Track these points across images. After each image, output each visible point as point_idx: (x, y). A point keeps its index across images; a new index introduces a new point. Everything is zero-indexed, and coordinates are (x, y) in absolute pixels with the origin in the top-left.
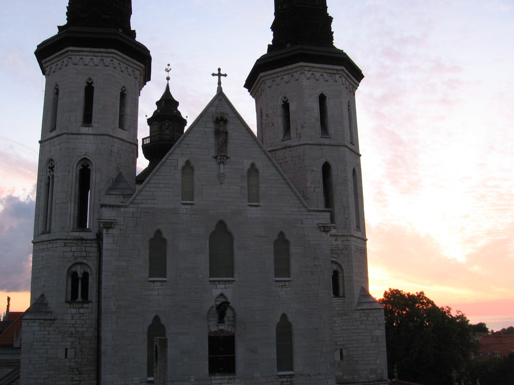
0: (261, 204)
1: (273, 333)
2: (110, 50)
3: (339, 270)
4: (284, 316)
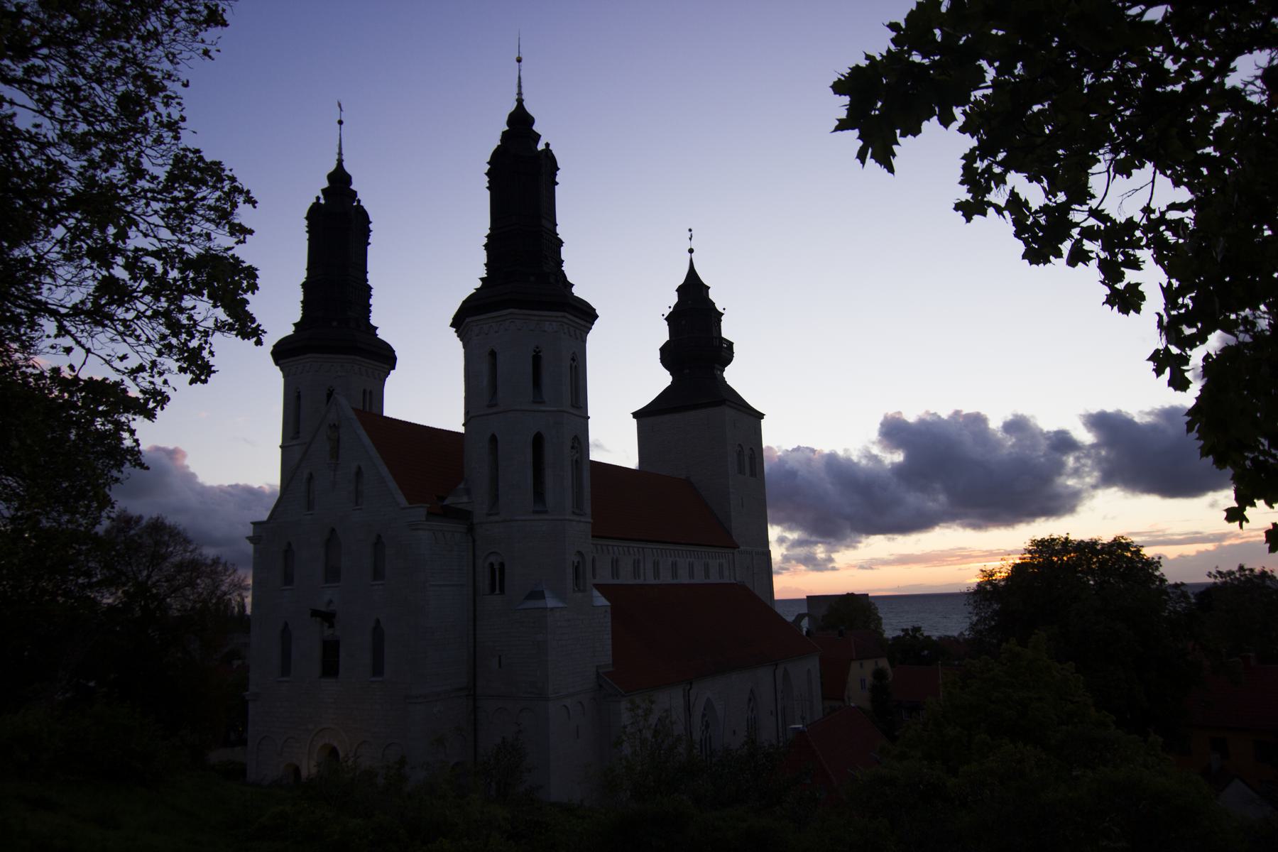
4: (378, 621)
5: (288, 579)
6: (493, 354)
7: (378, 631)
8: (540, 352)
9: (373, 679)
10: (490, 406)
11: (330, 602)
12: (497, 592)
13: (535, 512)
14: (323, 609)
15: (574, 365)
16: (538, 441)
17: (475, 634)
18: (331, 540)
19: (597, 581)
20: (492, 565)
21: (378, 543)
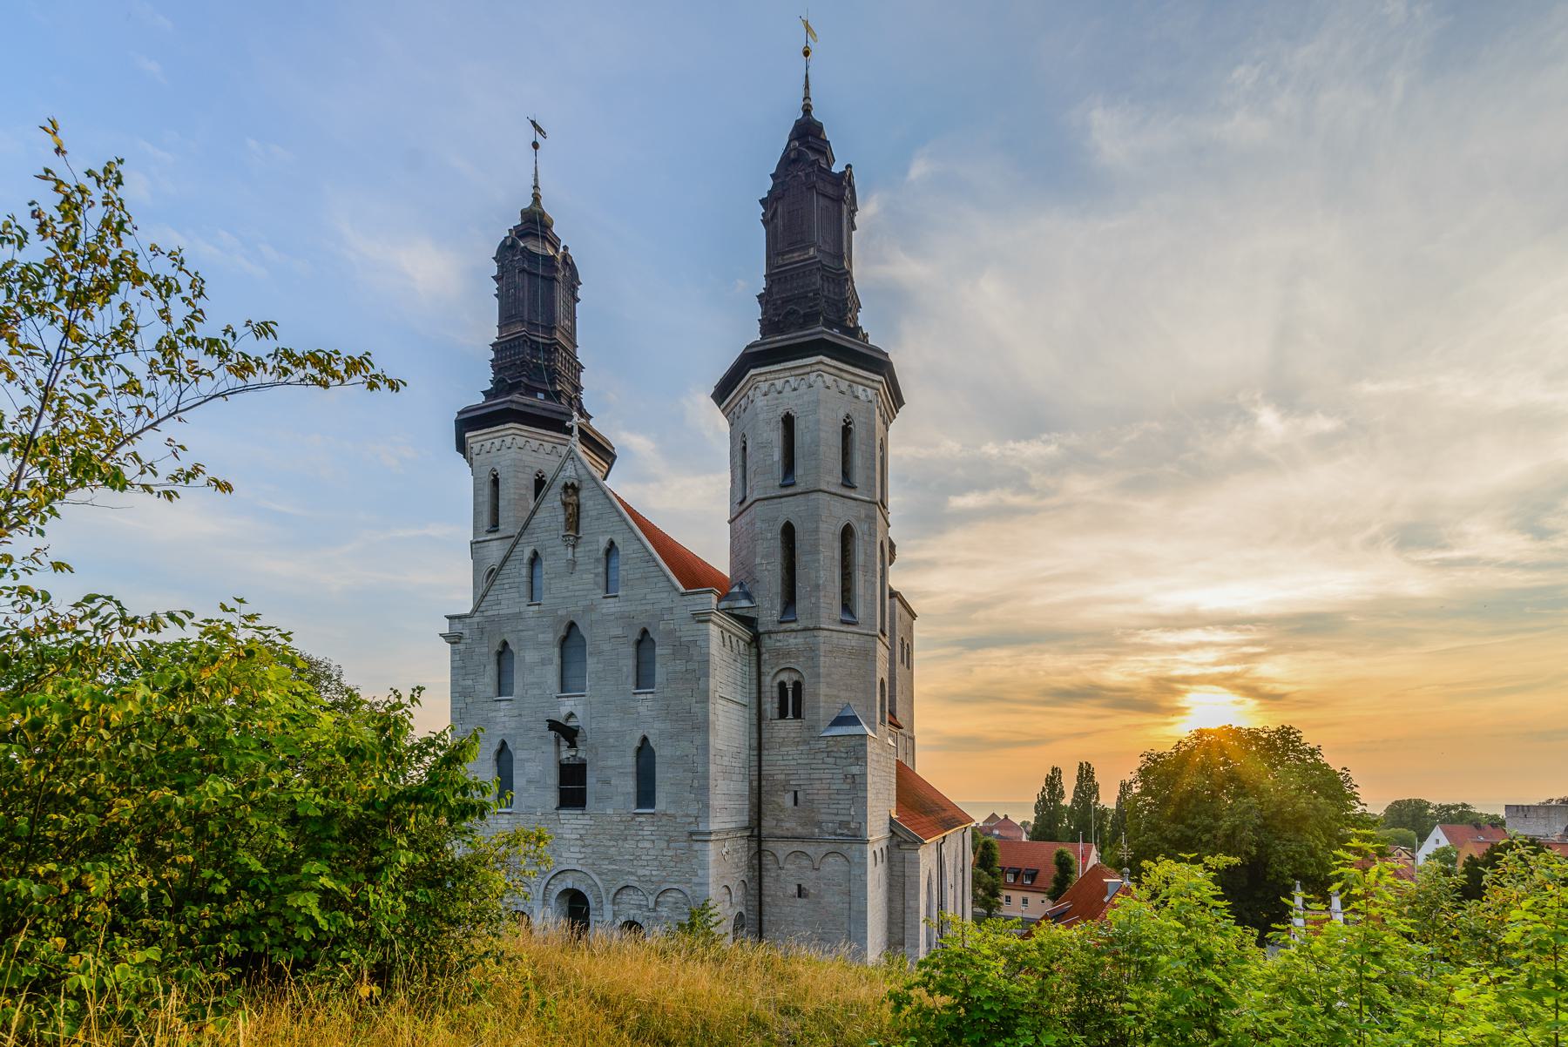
0: (620, 593)
1: (630, 759)
2: (507, 426)
3: (801, 680)
4: (645, 739)
5: (503, 686)
6: (788, 422)
7: (645, 753)
9: (637, 811)
10: (782, 486)
11: (571, 715)
12: (790, 715)
13: (843, 622)
16: (847, 534)
17: (760, 766)
18: (570, 639)
20: (782, 685)
21: (644, 641)
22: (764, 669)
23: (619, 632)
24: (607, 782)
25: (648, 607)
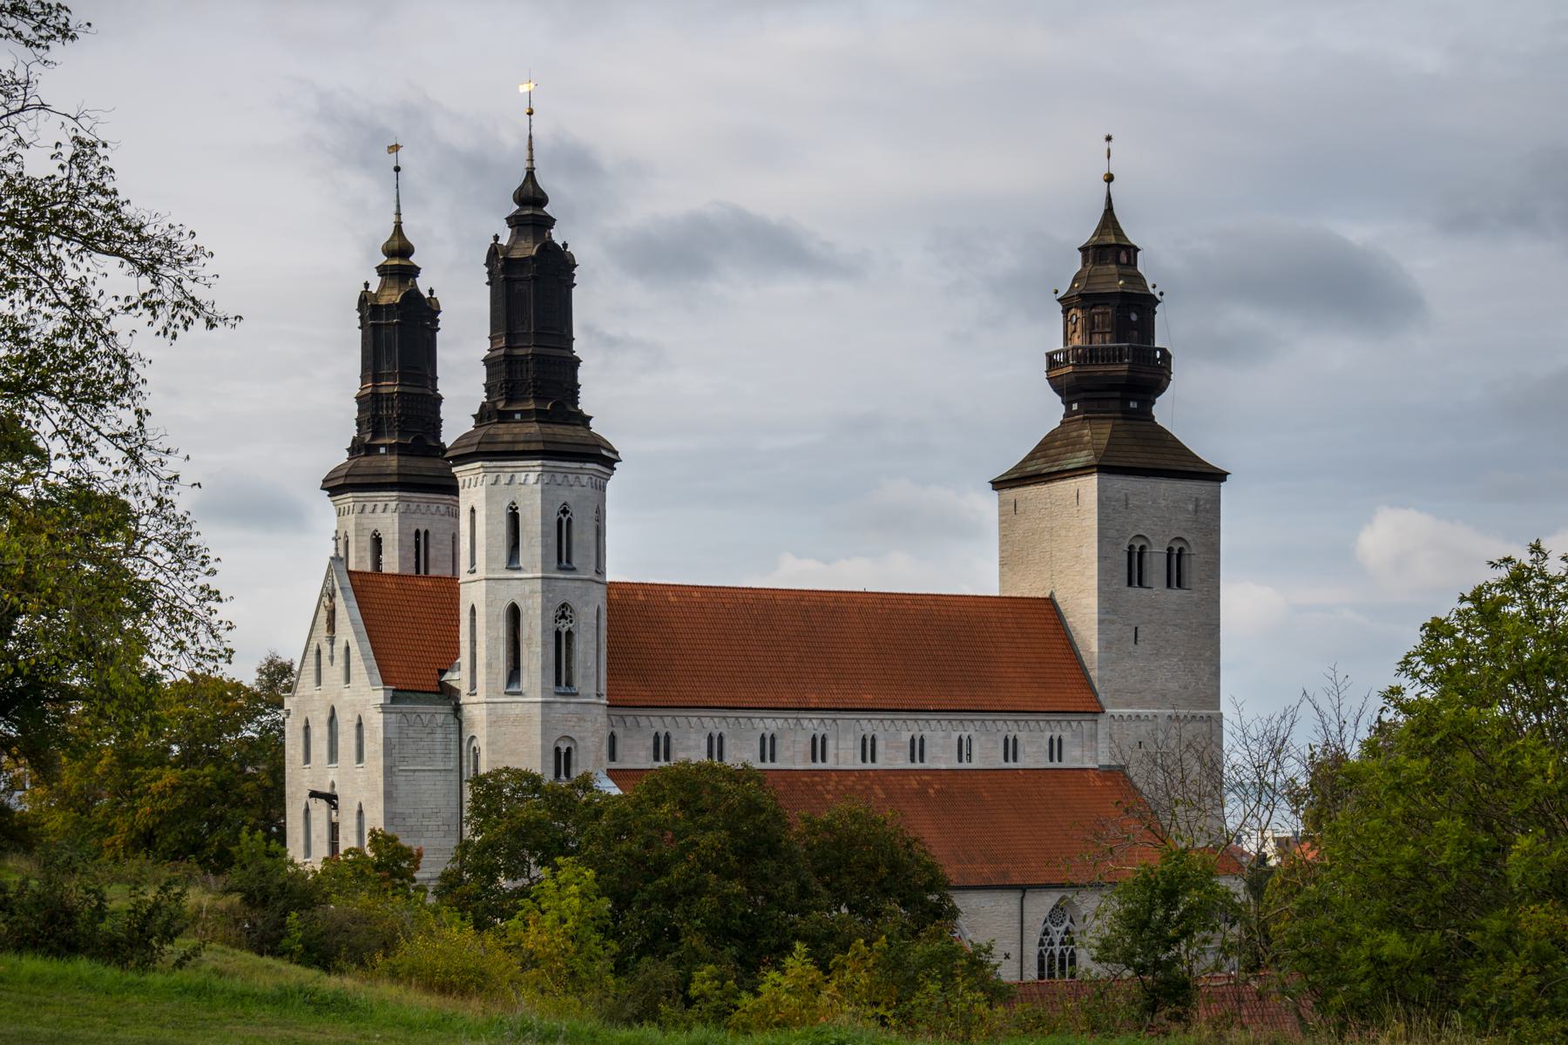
8: (517, 508)
14: (327, 790)
15: (565, 520)
19: (614, 765)
22: (464, 736)
23: (349, 716)
24: (346, 839)
25: (361, 698)
